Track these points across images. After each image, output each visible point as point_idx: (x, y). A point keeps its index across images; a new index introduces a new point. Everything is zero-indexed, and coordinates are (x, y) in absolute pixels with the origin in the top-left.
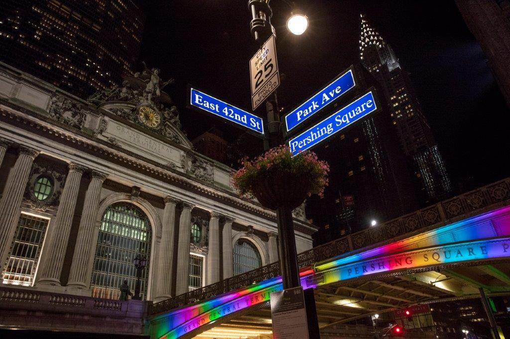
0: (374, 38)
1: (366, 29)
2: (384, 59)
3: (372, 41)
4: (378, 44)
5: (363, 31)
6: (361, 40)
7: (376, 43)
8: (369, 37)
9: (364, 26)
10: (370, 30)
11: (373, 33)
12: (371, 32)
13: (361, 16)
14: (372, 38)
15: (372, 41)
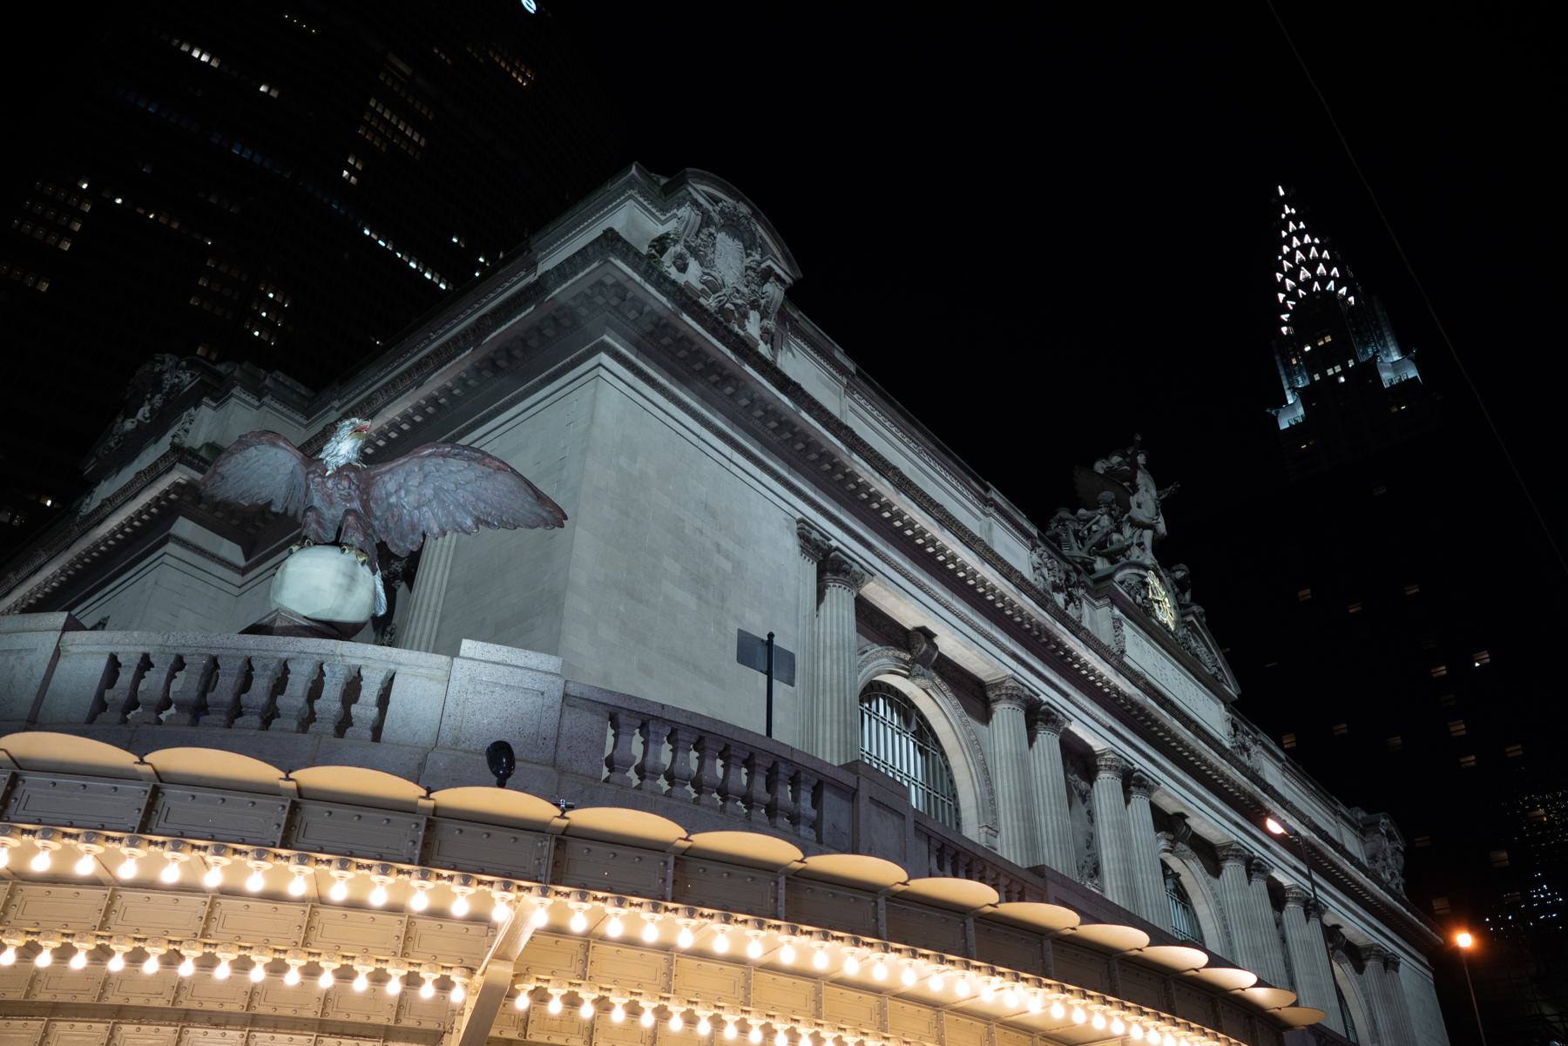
0: (1329, 270)
1: (1301, 239)
2: (1366, 344)
3: (1323, 281)
4: (1343, 291)
5: (1288, 241)
6: (1282, 271)
7: (1338, 287)
8: (1311, 265)
9: (1292, 226)
10: (1313, 244)
11: (1326, 254)
12: (1320, 249)
13: (1282, 193)
14: (1321, 269)
15: (1323, 281)
